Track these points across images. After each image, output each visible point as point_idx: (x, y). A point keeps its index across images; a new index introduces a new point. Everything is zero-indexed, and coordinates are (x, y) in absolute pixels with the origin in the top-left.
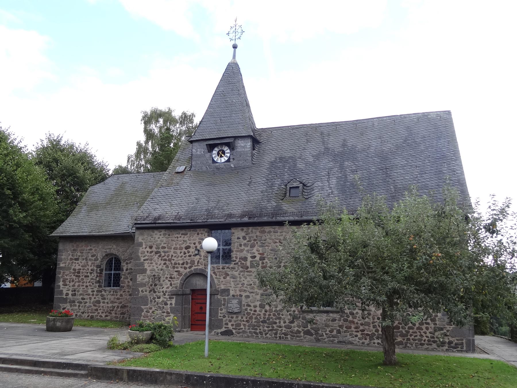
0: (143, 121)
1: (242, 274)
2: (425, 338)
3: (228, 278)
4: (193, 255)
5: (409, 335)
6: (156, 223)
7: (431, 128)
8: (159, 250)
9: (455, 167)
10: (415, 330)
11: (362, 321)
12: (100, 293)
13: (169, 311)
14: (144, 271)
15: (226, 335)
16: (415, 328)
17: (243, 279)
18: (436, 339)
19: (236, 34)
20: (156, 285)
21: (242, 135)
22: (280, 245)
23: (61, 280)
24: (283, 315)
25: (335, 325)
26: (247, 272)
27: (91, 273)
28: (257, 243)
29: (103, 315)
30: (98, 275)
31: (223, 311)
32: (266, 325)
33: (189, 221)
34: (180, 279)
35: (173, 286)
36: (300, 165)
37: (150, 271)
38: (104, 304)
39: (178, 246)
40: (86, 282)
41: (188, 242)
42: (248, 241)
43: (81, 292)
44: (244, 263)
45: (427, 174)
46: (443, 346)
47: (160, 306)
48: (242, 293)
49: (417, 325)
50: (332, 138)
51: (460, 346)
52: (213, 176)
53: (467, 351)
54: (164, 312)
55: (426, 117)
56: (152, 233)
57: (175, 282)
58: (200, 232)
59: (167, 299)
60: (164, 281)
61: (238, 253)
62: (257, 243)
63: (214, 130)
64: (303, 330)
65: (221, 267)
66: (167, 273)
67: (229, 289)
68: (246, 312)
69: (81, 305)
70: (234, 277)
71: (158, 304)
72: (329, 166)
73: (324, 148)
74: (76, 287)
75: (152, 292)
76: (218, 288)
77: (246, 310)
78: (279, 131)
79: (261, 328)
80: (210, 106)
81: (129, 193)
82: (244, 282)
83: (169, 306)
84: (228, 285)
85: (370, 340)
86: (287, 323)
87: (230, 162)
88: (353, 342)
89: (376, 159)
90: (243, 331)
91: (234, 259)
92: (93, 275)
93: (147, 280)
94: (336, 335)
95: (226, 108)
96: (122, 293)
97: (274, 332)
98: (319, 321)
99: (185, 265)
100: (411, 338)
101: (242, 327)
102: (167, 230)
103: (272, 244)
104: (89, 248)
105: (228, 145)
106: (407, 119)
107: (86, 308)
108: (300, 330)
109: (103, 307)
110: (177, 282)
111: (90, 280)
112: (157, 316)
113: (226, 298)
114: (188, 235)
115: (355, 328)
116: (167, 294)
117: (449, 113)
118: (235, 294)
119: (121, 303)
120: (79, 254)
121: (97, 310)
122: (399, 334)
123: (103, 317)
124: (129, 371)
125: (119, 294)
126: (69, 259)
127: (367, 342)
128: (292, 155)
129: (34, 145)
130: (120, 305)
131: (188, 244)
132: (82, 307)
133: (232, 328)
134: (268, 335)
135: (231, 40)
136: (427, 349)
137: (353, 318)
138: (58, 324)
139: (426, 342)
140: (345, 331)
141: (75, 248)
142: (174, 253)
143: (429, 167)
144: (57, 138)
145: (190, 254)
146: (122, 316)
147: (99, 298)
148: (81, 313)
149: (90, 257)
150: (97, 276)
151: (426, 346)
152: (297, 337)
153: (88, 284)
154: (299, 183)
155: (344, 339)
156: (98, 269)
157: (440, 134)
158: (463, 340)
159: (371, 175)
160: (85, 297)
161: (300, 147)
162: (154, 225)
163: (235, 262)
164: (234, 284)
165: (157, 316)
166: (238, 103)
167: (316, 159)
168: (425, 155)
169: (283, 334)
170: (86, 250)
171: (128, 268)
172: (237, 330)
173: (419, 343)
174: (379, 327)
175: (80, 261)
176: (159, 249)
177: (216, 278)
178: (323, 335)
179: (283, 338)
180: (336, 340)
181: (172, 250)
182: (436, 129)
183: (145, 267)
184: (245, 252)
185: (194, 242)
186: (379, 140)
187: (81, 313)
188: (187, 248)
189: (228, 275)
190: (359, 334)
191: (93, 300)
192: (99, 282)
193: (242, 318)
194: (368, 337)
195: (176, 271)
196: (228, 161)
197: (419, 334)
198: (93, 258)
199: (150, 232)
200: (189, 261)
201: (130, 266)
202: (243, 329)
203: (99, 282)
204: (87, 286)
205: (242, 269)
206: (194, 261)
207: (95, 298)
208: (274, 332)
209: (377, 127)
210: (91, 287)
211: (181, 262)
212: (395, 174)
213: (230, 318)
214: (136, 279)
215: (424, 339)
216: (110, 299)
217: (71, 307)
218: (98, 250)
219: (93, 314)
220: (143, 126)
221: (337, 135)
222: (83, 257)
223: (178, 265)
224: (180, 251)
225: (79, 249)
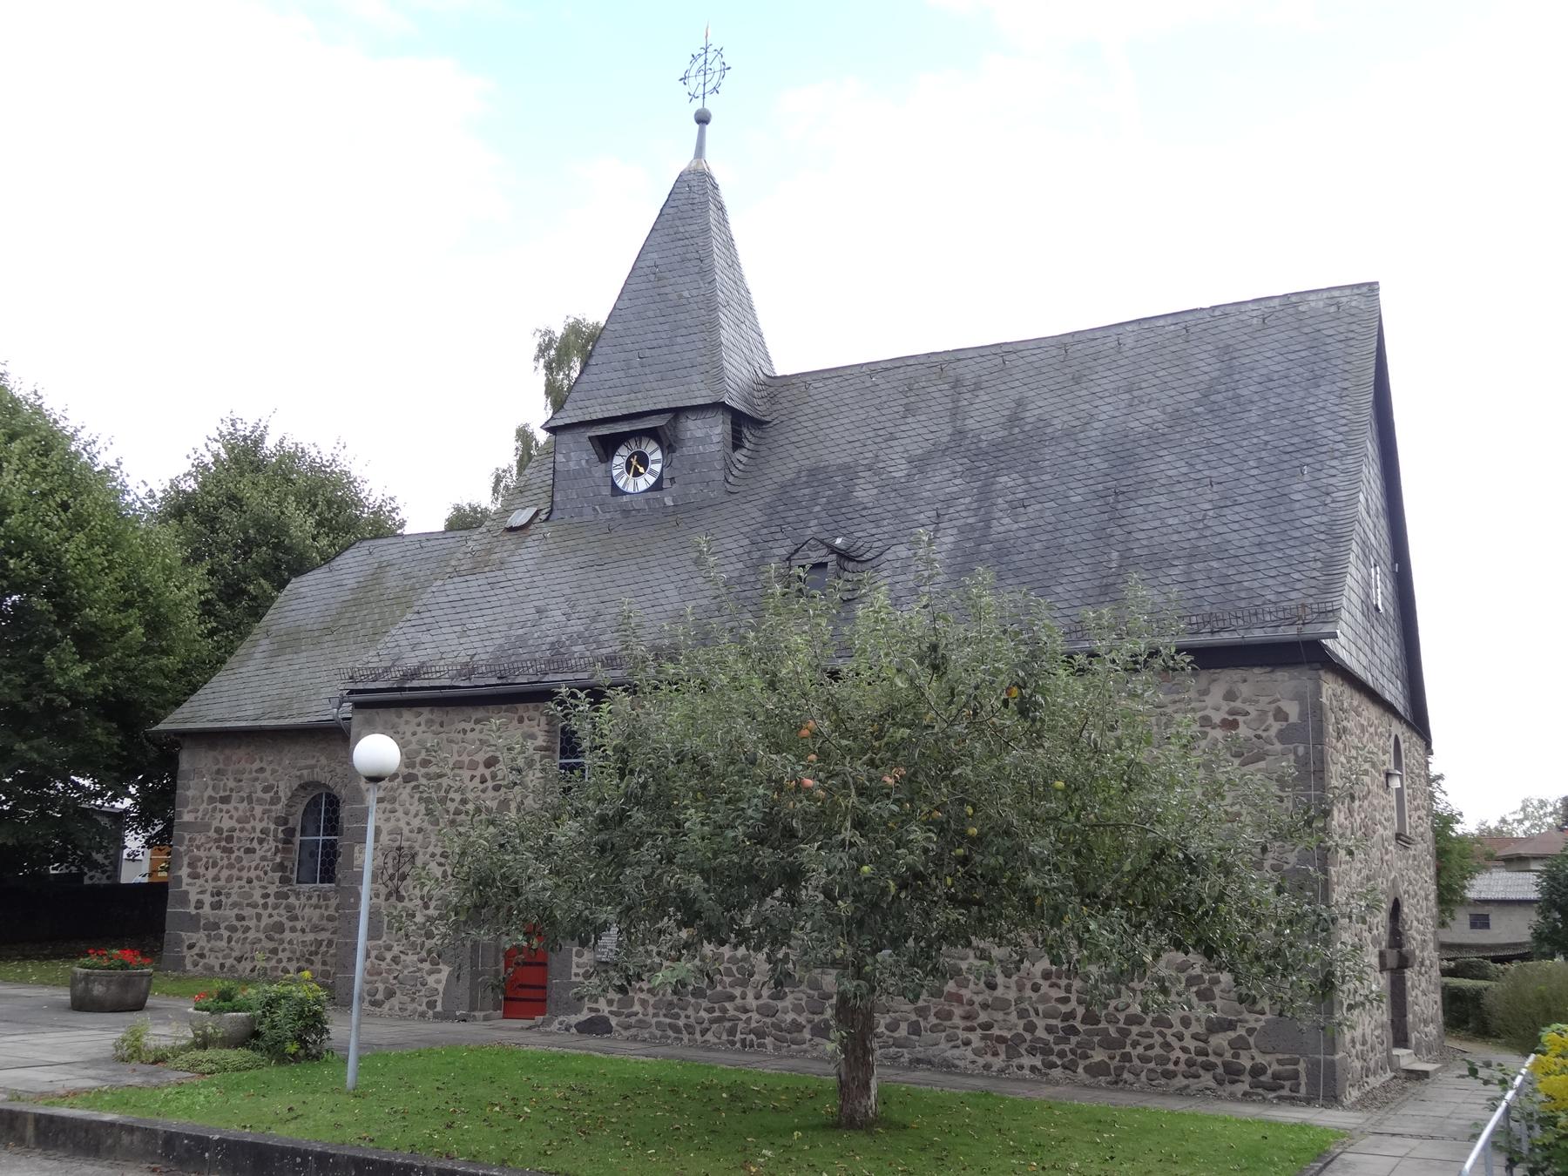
0: (542, 361)
5: (1129, 1042)
6: (404, 689)
7: (1298, 347)
8: (415, 771)
9: (1332, 481)
10: (1147, 1026)
11: (987, 996)
12: (284, 902)
15: (590, 1032)
16: (1149, 1020)
18: (1212, 1058)
19: (708, 77)
20: (403, 877)
21: (694, 403)
23: (186, 861)
27: (261, 841)
29: (292, 967)
32: (705, 1003)
33: (494, 681)
36: (864, 493)
37: (390, 833)
38: (293, 935)
39: (466, 759)
43: (234, 898)
45: (1237, 509)
46: (1233, 1082)
50: (986, 398)
51: (1287, 1084)
52: (605, 536)
53: (1309, 1101)
55: (1291, 311)
56: (397, 720)
63: (620, 390)
64: (809, 1022)
66: (433, 839)
69: (236, 936)
72: (947, 490)
73: (950, 431)
74: (222, 883)
75: (393, 899)
78: (830, 381)
79: (690, 1011)
81: (392, 596)
85: (1009, 1058)
86: (764, 1000)
87: (662, 489)
88: (957, 1062)
89: (1097, 460)
90: (640, 1021)
94: (906, 1038)
95: (662, 319)
97: (728, 1024)
100: (1134, 1053)
101: (637, 1008)
102: (436, 709)
104: (257, 765)
105: (653, 434)
106: (1232, 320)
107: (248, 946)
108: (802, 1020)
109: (290, 942)
111: (258, 861)
112: (406, 972)
116: (433, 904)
117: (1370, 290)
120: (231, 784)
121: (274, 951)
122: (1096, 1039)
124: (39, 1118)
126: (205, 798)
127: (998, 1062)
128: (848, 459)
129: (188, 457)
132: (237, 942)
134: (709, 1036)
135: (693, 96)
136: (1181, 1092)
137: (959, 985)
138: (98, 990)
139: (1182, 1066)
140: (935, 1025)
141: (221, 766)
143: (1252, 481)
144: (253, 432)
147: (280, 916)
149: (260, 794)
150: (277, 850)
151: (1180, 1081)
152: (794, 1042)
153: (253, 874)
154: (825, 551)
156: (281, 828)
157: (1324, 365)
158: (1296, 1062)
159: (1067, 517)
160: (247, 912)
161: (881, 432)
162: (397, 695)
166: (698, 299)
167: (914, 471)
168: (1255, 441)
169: (751, 1031)
170: (250, 772)
172: (622, 1018)
174: (1037, 1014)
175: (234, 803)
176: (413, 767)
179: (752, 1046)
180: (906, 1055)
182: (1314, 351)
186: (1127, 396)
188: (491, 762)
190: (975, 1037)
191: (265, 921)
192: (281, 867)
194: (1002, 1048)
196: (657, 486)
197: (1158, 1039)
198: (267, 796)
202: (640, 1016)
203: (281, 867)
204: (250, 881)
208: (728, 1024)
209: (1132, 353)
212: (1140, 510)
215: (1173, 1056)
217: (208, 941)
220: (541, 378)
221: (1003, 387)
224: (471, 773)
225: (230, 768)
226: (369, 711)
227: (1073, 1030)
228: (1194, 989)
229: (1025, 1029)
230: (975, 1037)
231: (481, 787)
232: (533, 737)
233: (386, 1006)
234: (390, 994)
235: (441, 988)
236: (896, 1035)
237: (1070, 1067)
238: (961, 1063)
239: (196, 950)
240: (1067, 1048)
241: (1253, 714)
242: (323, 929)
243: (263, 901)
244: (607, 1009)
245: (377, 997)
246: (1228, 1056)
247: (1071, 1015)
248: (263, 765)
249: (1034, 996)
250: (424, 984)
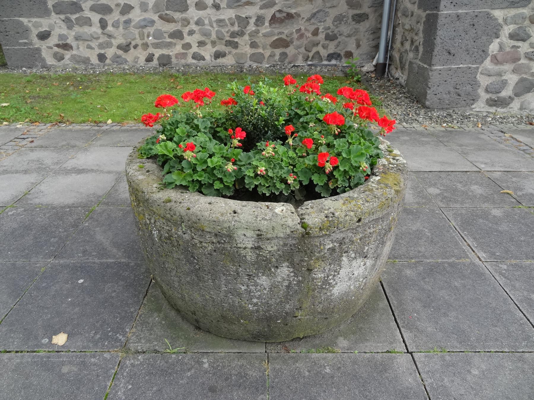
29: (207, 53)
69: (110, 19)
109: (198, 23)
121: (177, 35)
123: (208, 57)
130: (269, 13)
132: (116, 25)
148: (119, 47)
187: (119, 47)
239: (53, 40)
245: (504, 94)
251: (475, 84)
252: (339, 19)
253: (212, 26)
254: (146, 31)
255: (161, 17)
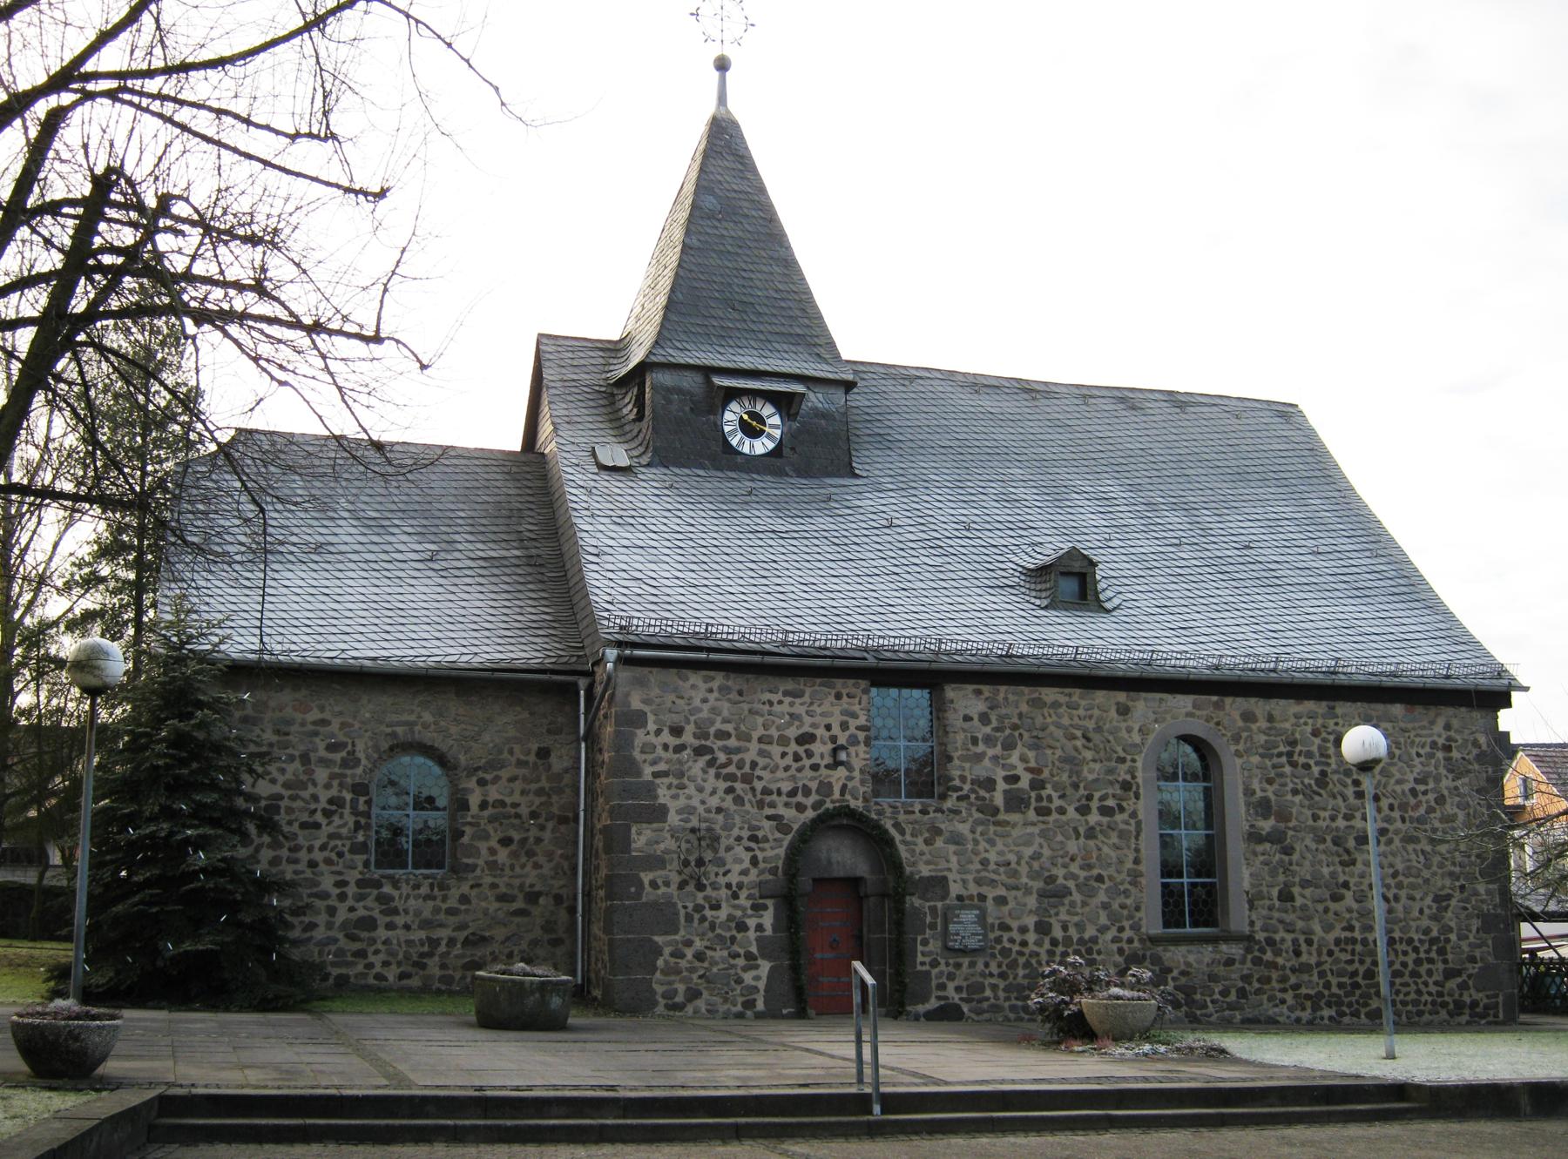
1: (979, 829)
2: (1426, 997)
3: (939, 843)
4: (827, 767)
8: (708, 743)
11: (1294, 962)
12: (375, 892)
13: (754, 949)
14: (660, 813)
17: (983, 845)
18: (1447, 998)
22: (1084, 747)
24: (1099, 953)
25: (1233, 976)
26: (995, 824)
28: (1021, 735)
29: (391, 974)
30: (363, 821)
31: (930, 947)
34: (786, 843)
35: (762, 865)
37: (679, 812)
40: (310, 849)
41: (807, 720)
42: (997, 729)
44: (987, 795)
47: (723, 933)
48: (984, 890)
49: (1411, 966)
51: (1491, 1012)
54: (736, 956)
56: (681, 683)
57: (770, 853)
58: (844, 692)
59: (744, 909)
60: (729, 849)
61: (967, 765)
62: (1021, 735)
65: (917, 808)
66: (737, 820)
67: (945, 878)
68: (999, 947)
70: (956, 839)
71: (713, 927)
75: (691, 888)
76: (912, 873)
77: (998, 940)
80: (788, 265)
82: (986, 855)
83: (752, 934)
84: (943, 865)
91: (957, 783)
92: (337, 820)
93: (670, 844)
96: (465, 889)
98: (1195, 965)
99: (800, 798)
101: (988, 993)
103: (1064, 741)
110: (775, 852)
112: (715, 970)
113: (939, 905)
114: (807, 698)
115: (1279, 982)
116: (743, 894)
118: (964, 893)
119: (462, 927)
120: (269, 736)
121: (361, 954)
123: (391, 978)
125: (455, 893)
130: (462, 936)
131: (806, 729)
133: (961, 999)
139: (1429, 1006)
142: (762, 753)
145: (813, 761)
146: (469, 974)
149: (322, 753)
150: (358, 826)
151: (1427, 1017)
153: (318, 856)
155: (1256, 1013)
158: (1496, 996)
163: (960, 793)
164: (959, 862)
165: (715, 970)
171: (491, 799)
173: (1414, 1010)
176: (706, 736)
177: (904, 842)
178: (1205, 1006)
181: (754, 746)
183: (661, 800)
184: (986, 762)
185: (827, 721)
188: (806, 739)
189: (938, 832)
190: (1289, 996)
191: (342, 915)
193: (987, 965)
194: (1308, 1004)
195: (769, 818)
197: (1413, 987)
198: (338, 757)
199: (671, 675)
200: (814, 785)
201: (494, 794)
205: (980, 815)
206: (830, 785)
207: (352, 909)
210: (334, 868)
211: (786, 787)
213: (951, 969)
214: (627, 841)
215: (1423, 999)
216: (418, 913)
218: (357, 725)
219: (343, 971)
222: (290, 751)
223: (774, 797)
226: (646, 670)
227: (1356, 986)
228: (1435, 948)
229: (1324, 987)
230: (1289, 996)
231: (795, 765)
232: (854, 716)
233: (690, 1009)
234: (693, 994)
235: (761, 985)
236: (1228, 1000)
237: (1356, 1014)
238: (1281, 1019)
240: (1354, 999)
241: (1460, 741)
242: (441, 925)
243: (338, 891)
244: (957, 997)
246: (1457, 996)
247: (1354, 974)
248: (327, 715)
249: (1330, 960)
250: (739, 981)
251: (654, 992)
252: (534, 943)
253: (400, 946)
254: (326, 950)
255: (347, 936)
